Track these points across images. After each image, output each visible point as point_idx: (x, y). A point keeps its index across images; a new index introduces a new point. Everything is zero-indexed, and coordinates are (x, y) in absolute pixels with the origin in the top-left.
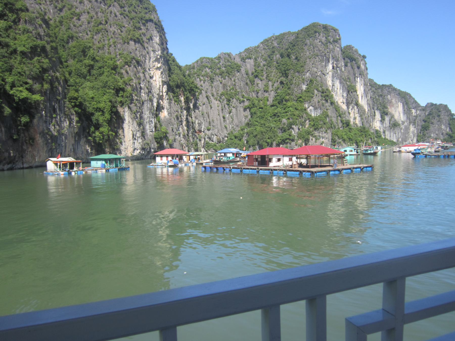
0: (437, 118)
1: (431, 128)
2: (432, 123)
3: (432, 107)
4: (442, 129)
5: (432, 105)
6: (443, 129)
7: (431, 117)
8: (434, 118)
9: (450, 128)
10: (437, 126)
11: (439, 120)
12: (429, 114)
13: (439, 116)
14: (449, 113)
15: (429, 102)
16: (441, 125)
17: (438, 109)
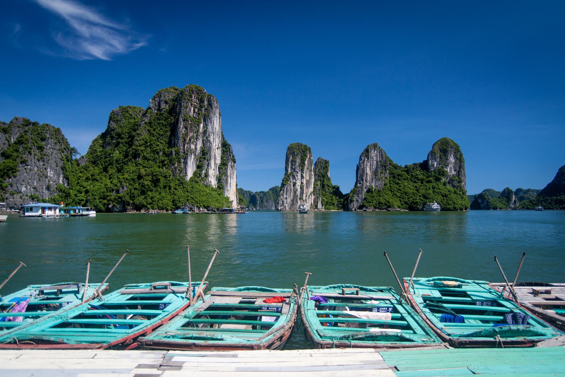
0: (35, 151)
1: (22, 173)
2: (23, 162)
3: (26, 128)
4: (46, 177)
5: (27, 123)
6: (50, 177)
7: (21, 149)
8: (30, 152)
9: (66, 178)
10: (36, 169)
11: (41, 158)
12: (19, 142)
13: (41, 148)
14: (63, 146)
15: (20, 116)
16: (46, 169)
17: (39, 134)
